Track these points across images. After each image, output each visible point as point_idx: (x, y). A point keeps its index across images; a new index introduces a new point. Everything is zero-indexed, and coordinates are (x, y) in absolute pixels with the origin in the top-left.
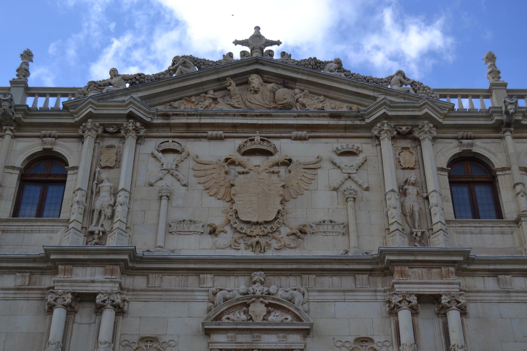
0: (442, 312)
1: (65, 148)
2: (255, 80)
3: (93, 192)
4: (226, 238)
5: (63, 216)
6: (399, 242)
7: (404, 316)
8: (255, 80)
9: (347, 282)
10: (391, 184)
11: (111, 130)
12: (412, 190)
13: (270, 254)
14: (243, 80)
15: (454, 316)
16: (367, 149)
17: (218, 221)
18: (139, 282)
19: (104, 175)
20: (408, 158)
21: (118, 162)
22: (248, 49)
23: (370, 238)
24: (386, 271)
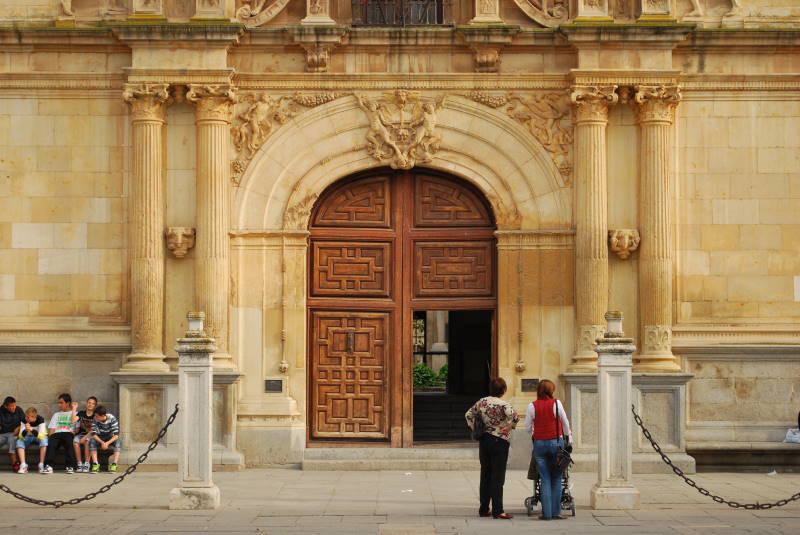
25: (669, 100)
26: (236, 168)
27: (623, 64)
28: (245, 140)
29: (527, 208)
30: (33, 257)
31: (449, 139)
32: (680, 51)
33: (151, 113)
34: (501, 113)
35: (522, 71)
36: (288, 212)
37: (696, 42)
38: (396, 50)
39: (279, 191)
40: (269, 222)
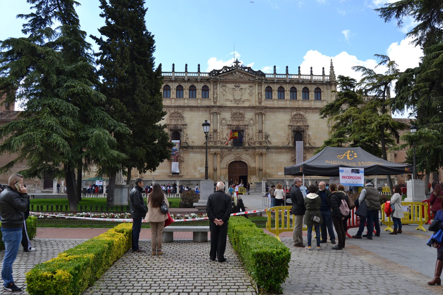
0: (262, 115)
1: (208, 85)
2: (237, 72)
3: (214, 94)
4: (233, 102)
5: (210, 98)
6: (257, 104)
7: (257, 116)
8: (237, 72)
9: (250, 110)
10: (257, 94)
11: (216, 82)
12: (260, 94)
13: (239, 105)
14: (235, 72)
15: (264, 116)
16: (254, 86)
17: (232, 99)
18: (222, 109)
19: (215, 91)
20: (260, 88)
21: (217, 88)
22: (235, 64)
23: (254, 102)
24: (256, 108)
25: (265, 154)
26: (221, 161)
27: (261, 150)
28: (222, 158)
29: (251, 165)
30: (200, 170)
31: (243, 158)
32: (266, 149)
33: (212, 155)
34: (248, 155)
35: (250, 151)
36: (226, 165)
37: (268, 148)
38: (238, 149)
39: (226, 164)
40: (225, 166)
